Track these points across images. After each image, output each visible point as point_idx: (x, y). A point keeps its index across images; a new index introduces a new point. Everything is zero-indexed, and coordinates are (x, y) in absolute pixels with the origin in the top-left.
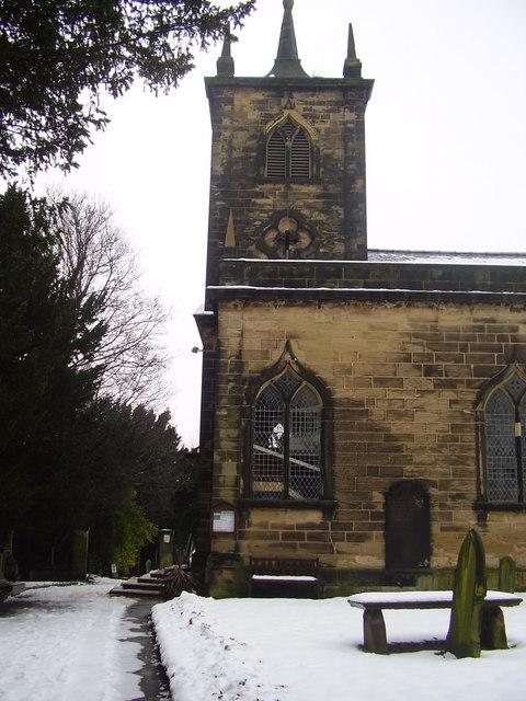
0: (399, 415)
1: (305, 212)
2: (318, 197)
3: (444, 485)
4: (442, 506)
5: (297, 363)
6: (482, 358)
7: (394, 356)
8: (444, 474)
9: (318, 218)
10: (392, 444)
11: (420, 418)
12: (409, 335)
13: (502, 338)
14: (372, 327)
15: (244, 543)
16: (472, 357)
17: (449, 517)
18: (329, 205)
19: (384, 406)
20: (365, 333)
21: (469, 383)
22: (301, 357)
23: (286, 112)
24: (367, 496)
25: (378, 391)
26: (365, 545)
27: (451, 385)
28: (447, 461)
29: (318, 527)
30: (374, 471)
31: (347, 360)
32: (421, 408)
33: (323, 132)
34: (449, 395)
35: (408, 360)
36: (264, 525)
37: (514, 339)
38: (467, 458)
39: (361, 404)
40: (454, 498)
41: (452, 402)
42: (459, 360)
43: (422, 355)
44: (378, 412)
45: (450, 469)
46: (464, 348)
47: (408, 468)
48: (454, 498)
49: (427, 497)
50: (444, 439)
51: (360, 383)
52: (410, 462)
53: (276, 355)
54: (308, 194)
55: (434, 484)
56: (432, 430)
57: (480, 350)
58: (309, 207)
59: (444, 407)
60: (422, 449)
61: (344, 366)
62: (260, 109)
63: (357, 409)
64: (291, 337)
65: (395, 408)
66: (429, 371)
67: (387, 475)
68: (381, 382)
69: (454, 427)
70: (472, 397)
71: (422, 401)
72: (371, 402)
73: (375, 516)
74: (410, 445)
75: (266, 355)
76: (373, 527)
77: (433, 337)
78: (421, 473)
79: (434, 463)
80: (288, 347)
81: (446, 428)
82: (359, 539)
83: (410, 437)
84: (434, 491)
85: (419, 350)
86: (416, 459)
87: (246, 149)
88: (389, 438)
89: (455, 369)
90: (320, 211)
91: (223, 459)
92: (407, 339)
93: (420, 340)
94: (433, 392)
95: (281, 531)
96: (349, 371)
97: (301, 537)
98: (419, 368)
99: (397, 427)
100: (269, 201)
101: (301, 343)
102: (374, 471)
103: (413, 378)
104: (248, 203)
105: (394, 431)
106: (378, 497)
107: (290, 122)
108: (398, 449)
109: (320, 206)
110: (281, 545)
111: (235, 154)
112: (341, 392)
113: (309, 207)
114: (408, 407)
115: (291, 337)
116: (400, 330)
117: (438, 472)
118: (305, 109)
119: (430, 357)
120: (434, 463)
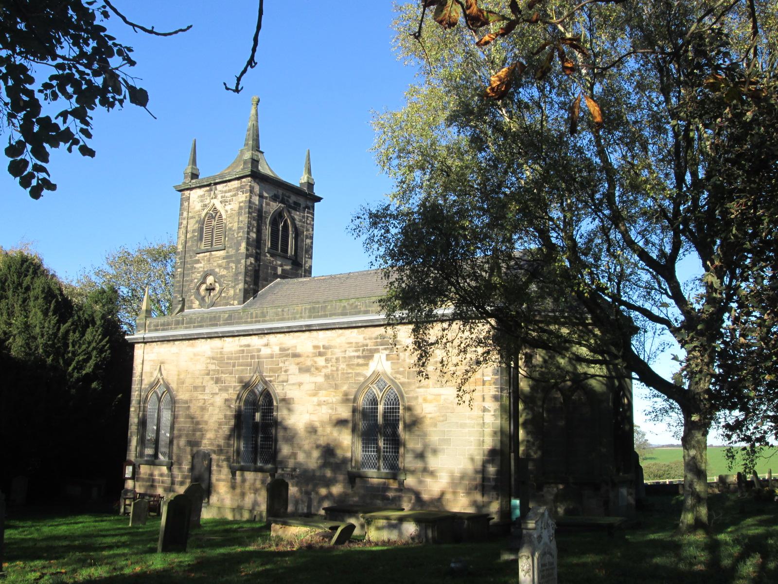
1: (217, 270)
2: (224, 258)
5: (163, 379)
6: (242, 371)
7: (203, 372)
9: (223, 273)
12: (210, 358)
13: (252, 357)
16: (237, 370)
20: (191, 359)
27: (225, 389)
33: (229, 212)
35: (208, 374)
37: (259, 357)
42: (231, 373)
43: (214, 370)
46: (234, 366)
54: (219, 257)
57: (241, 366)
58: (220, 266)
66: (217, 381)
85: (213, 367)
87: (194, 231)
89: (229, 379)
90: (225, 268)
92: (208, 361)
93: (215, 361)
94: (217, 394)
98: (212, 379)
100: (201, 265)
104: (193, 268)
109: (224, 265)
113: (220, 266)
114: (207, 403)
115: (162, 363)
118: (222, 197)
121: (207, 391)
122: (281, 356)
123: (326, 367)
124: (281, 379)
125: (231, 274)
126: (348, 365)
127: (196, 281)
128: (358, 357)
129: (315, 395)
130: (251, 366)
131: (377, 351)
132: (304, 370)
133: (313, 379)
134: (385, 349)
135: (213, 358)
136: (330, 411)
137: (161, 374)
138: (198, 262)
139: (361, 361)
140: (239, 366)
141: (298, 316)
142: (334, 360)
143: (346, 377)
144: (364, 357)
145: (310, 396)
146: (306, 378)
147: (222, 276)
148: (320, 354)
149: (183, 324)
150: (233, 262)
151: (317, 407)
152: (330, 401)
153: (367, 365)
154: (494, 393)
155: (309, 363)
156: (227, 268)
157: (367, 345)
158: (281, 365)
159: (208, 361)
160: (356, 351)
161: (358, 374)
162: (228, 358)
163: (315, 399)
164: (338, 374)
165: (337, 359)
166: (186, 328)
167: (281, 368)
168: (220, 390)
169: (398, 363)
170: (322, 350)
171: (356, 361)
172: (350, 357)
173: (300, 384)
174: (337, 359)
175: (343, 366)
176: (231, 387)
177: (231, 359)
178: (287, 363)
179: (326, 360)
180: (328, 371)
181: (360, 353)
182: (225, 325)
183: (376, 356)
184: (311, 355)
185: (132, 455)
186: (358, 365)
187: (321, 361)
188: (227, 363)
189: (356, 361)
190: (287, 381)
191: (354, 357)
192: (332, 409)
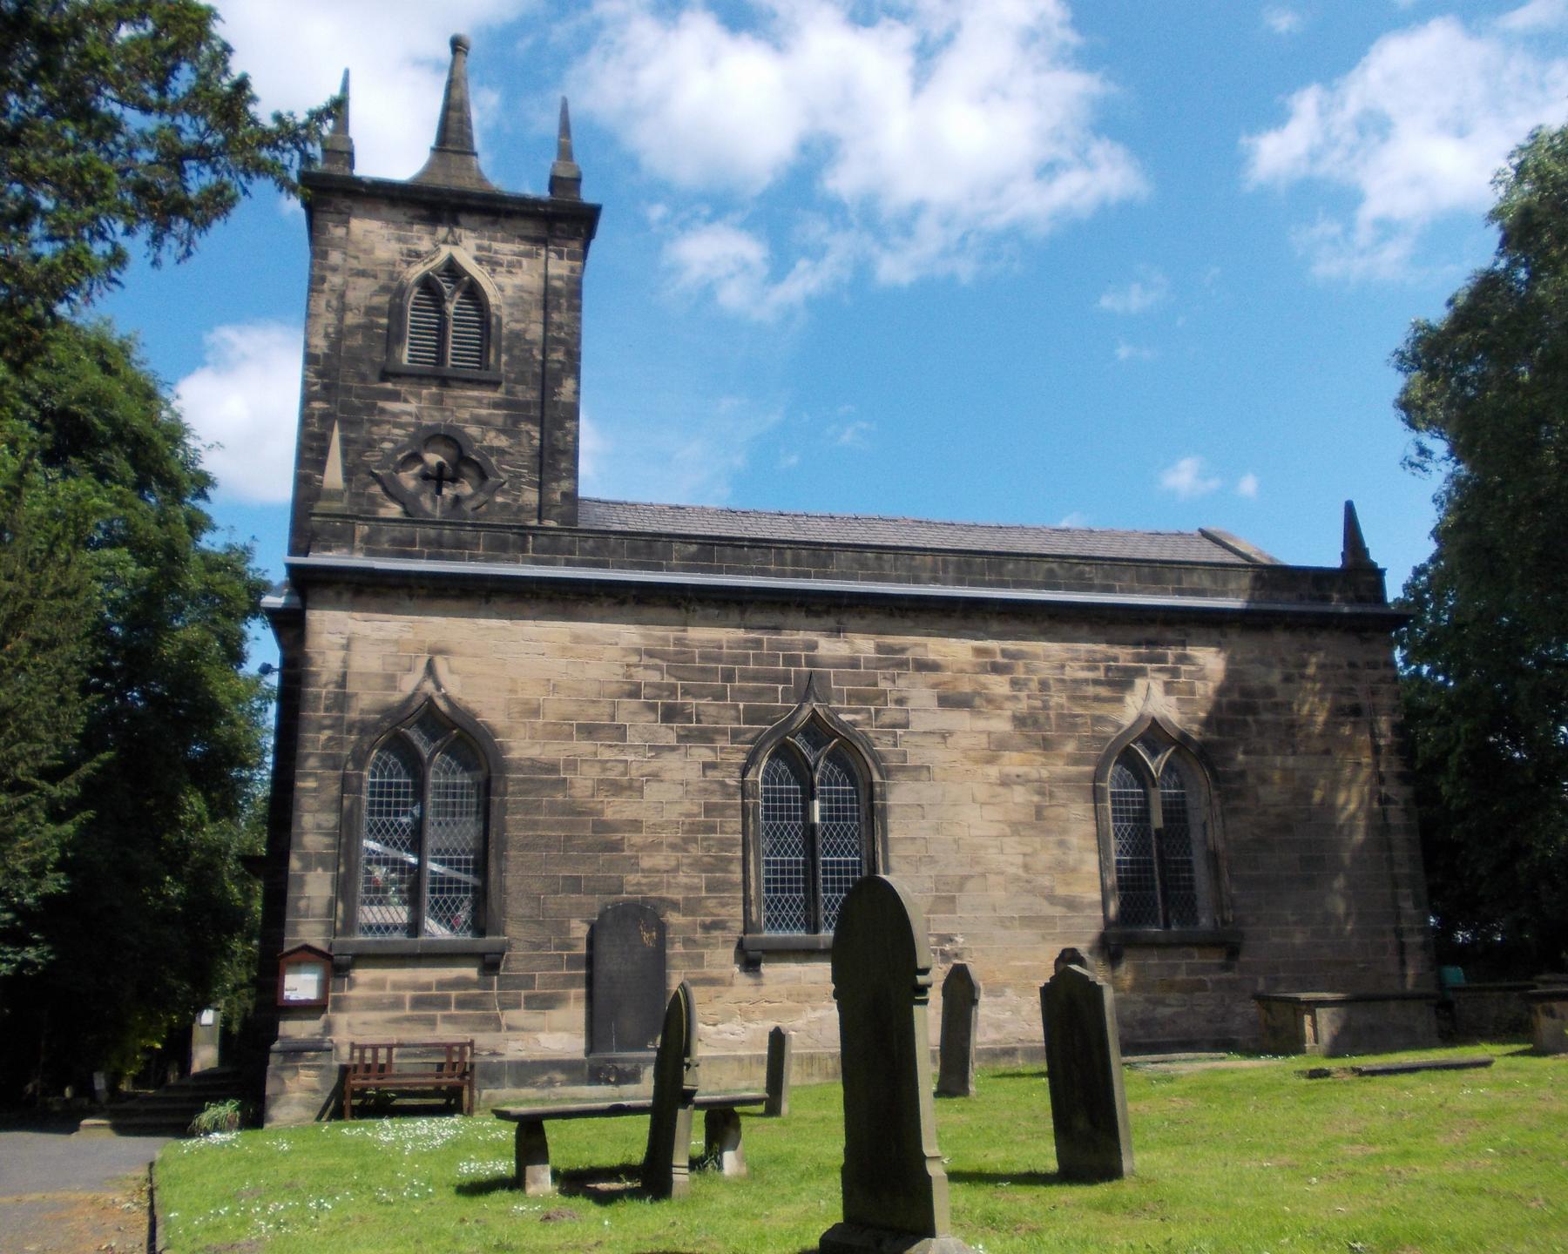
0: (616, 788)
1: (473, 430)
2: (496, 405)
3: (690, 907)
4: (688, 942)
5: (446, 698)
6: (758, 693)
7: (614, 687)
8: (689, 888)
9: (496, 443)
10: (608, 840)
11: (652, 792)
12: (638, 651)
13: (791, 660)
14: (577, 639)
15: (341, 1019)
16: (741, 690)
17: (698, 960)
18: (516, 422)
19: (594, 772)
20: (564, 649)
21: (736, 735)
22: (453, 686)
23: (445, 251)
24: (561, 928)
25: (584, 747)
26: (557, 1016)
27: (705, 737)
28: (697, 865)
29: (476, 984)
30: (574, 885)
31: (533, 693)
32: (655, 776)
34: (703, 753)
35: (634, 693)
36: (379, 984)
37: (811, 662)
38: (730, 860)
39: (552, 768)
40: (707, 928)
41: (707, 766)
42: (719, 695)
43: (658, 686)
44: (582, 784)
45: (700, 880)
46: (728, 676)
47: (632, 878)
48: (707, 928)
49: (662, 928)
50: (694, 828)
51: (556, 732)
52: (634, 866)
53: (408, 684)
54: (479, 400)
55: (674, 905)
56: (673, 813)
59: (693, 774)
60: (655, 846)
61: (526, 702)
62: (400, 240)
63: (548, 775)
64: (441, 652)
65: (611, 775)
66: (670, 714)
67: (593, 892)
68: (589, 731)
69: (709, 809)
70: (740, 758)
71: (655, 765)
72: (572, 765)
73: (573, 962)
74: (636, 838)
75: (391, 681)
76: (570, 982)
77: (679, 661)
78: (654, 886)
79: (676, 869)
80: (430, 670)
81: (695, 809)
82: (546, 1003)
83: (636, 825)
84: (674, 918)
85: (655, 677)
86: (646, 863)
87: (371, 311)
88: (603, 826)
89: (712, 711)
91: (307, 867)
92: (634, 659)
93: (658, 662)
94: (673, 749)
95: (408, 995)
96: (536, 712)
97: (444, 1003)
98: (652, 708)
99: (616, 809)
100: (412, 407)
101: (456, 662)
102: (574, 885)
103: (642, 725)
105: (609, 815)
106: (579, 930)
107: (452, 269)
108: (615, 847)
109: (499, 422)
110: (409, 1019)
111: (351, 319)
112: (521, 747)
114: (634, 773)
115: (441, 652)
116: (623, 643)
117: (686, 882)
119: (672, 690)
120: (676, 869)
121: (633, 738)
122: (879, 664)
123: (1016, 698)
124: (886, 718)
125: (528, 451)
126: (1072, 698)
127: (387, 445)
128: (1096, 682)
129: (990, 761)
130: (787, 680)
131: (1141, 672)
132: (949, 701)
133: (981, 724)
134: (1160, 670)
135: (650, 654)
136: (1036, 798)
137: (438, 687)
138: (395, 396)
139: (1104, 691)
140: (743, 678)
141: (925, 575)
142: (1034, 685)
143: (1068, 723)
144: (1109, 683)
145: (976, 761)
146: (958, 720)
147: (492, 450)
148: (996, 669)
149: (524, 549)
150: (529, 420)
151: (1000, 790)
152: (1034, 775)
153: (1120, 700)
154: (1400, 769)
155: (966, 687)
156: (509, 430)
157: (1115, 659)
158: (884, 685)
159: (634, 659)
160: (1090, 669)
161: (1098, 720)
162: (705, 657)
163: (993, 771)
164: (1048, 717)
165: (1044, 685)
166: (536, 562)
167: (884, 693)
168: (680, 738)
169: (1192, 701)
170: (999, 659)
171: (1091, 690)
172: (1075, 681)
173: (944, 735)
174: (1044, 685)
175: (1058, 699)
176: (723, 732)
177: (718, 659)
178: (901, 683)
179: (1014, 683)
180: (1023, 706)
181: (1100, 674)
182: (687, 569)
183: (1140, 683)
184: (968, 668)
185: (309, 931)
186: (1097, 699)
187: (999, 685)
188: (703, 670)
189: (1091, 690)
190: (906, 725)
191: (1086, 681)
192: (1041, 793)
